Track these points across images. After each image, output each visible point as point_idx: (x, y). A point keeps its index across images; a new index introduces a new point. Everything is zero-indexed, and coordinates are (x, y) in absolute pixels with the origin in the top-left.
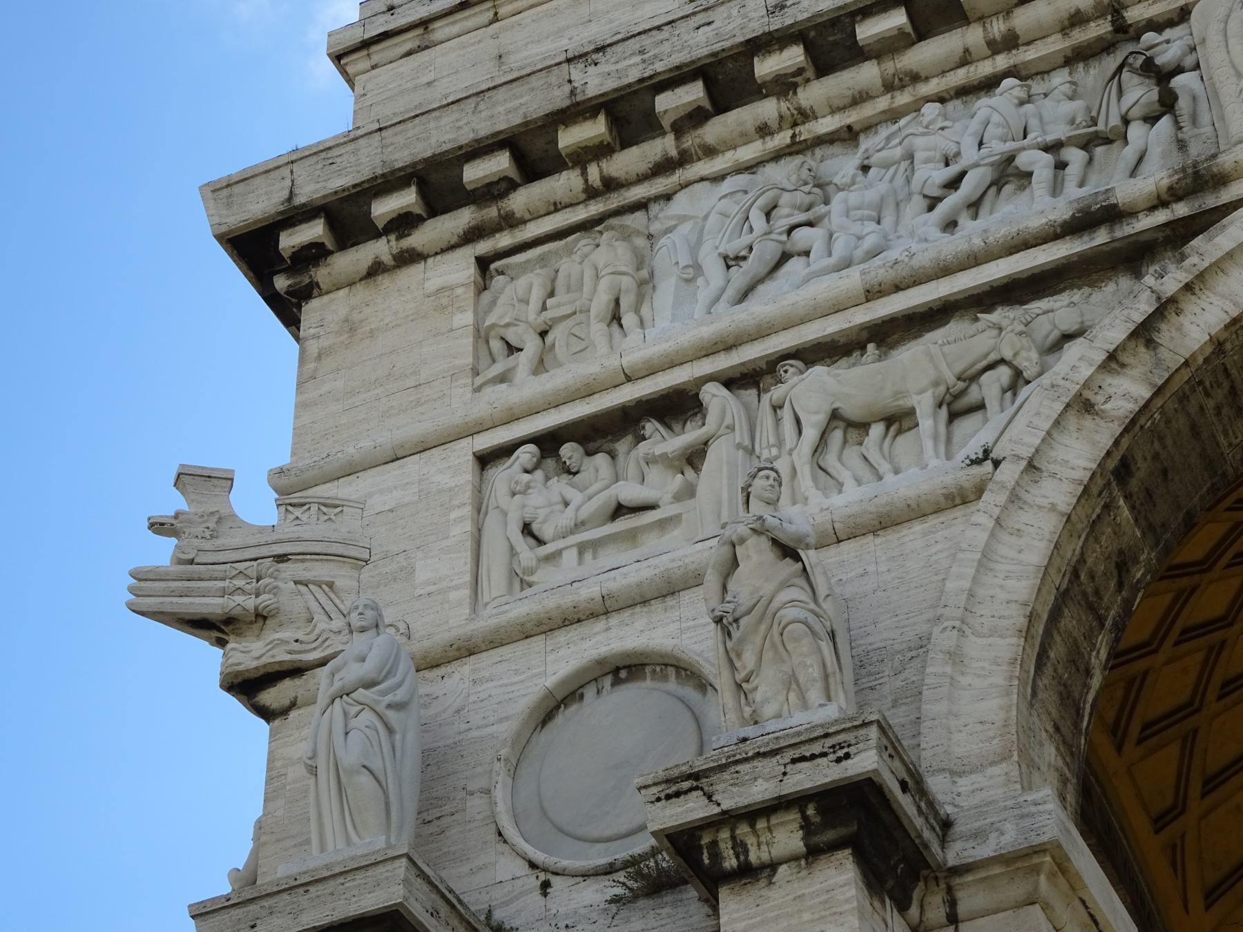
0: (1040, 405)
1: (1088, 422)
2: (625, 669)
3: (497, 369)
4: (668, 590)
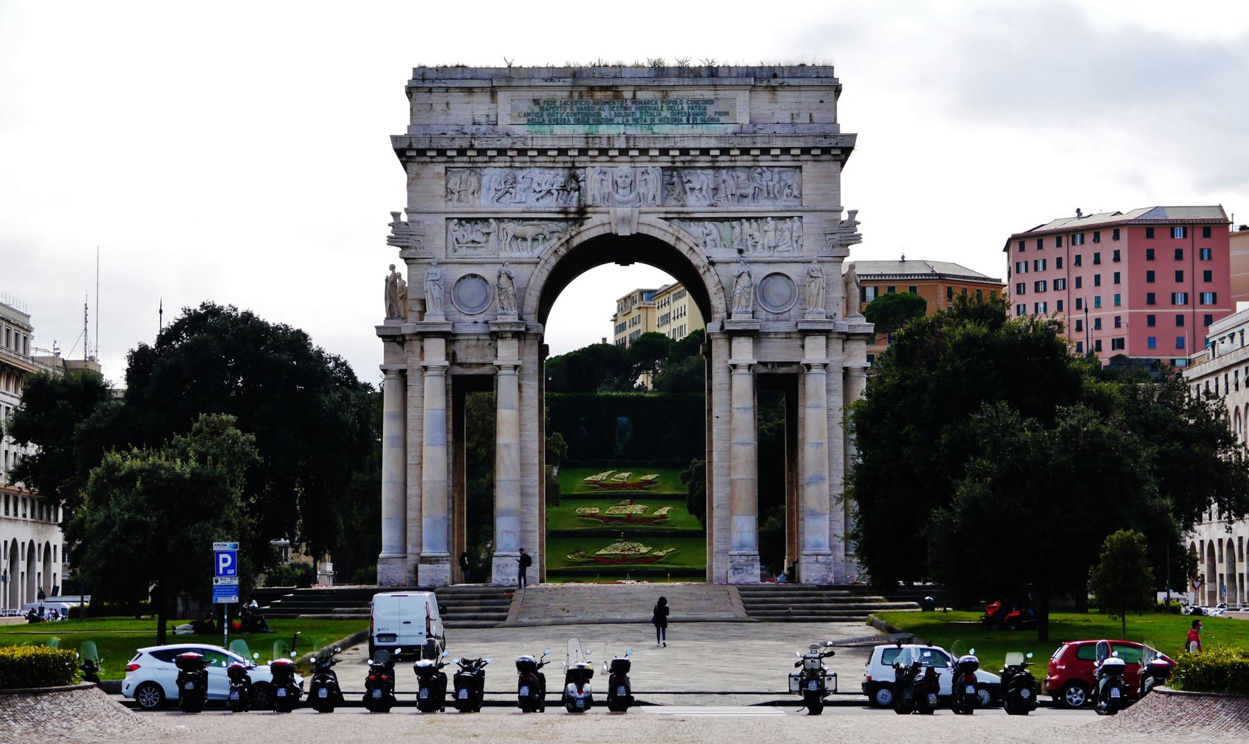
2: (474, 276)
4: (482, 263)
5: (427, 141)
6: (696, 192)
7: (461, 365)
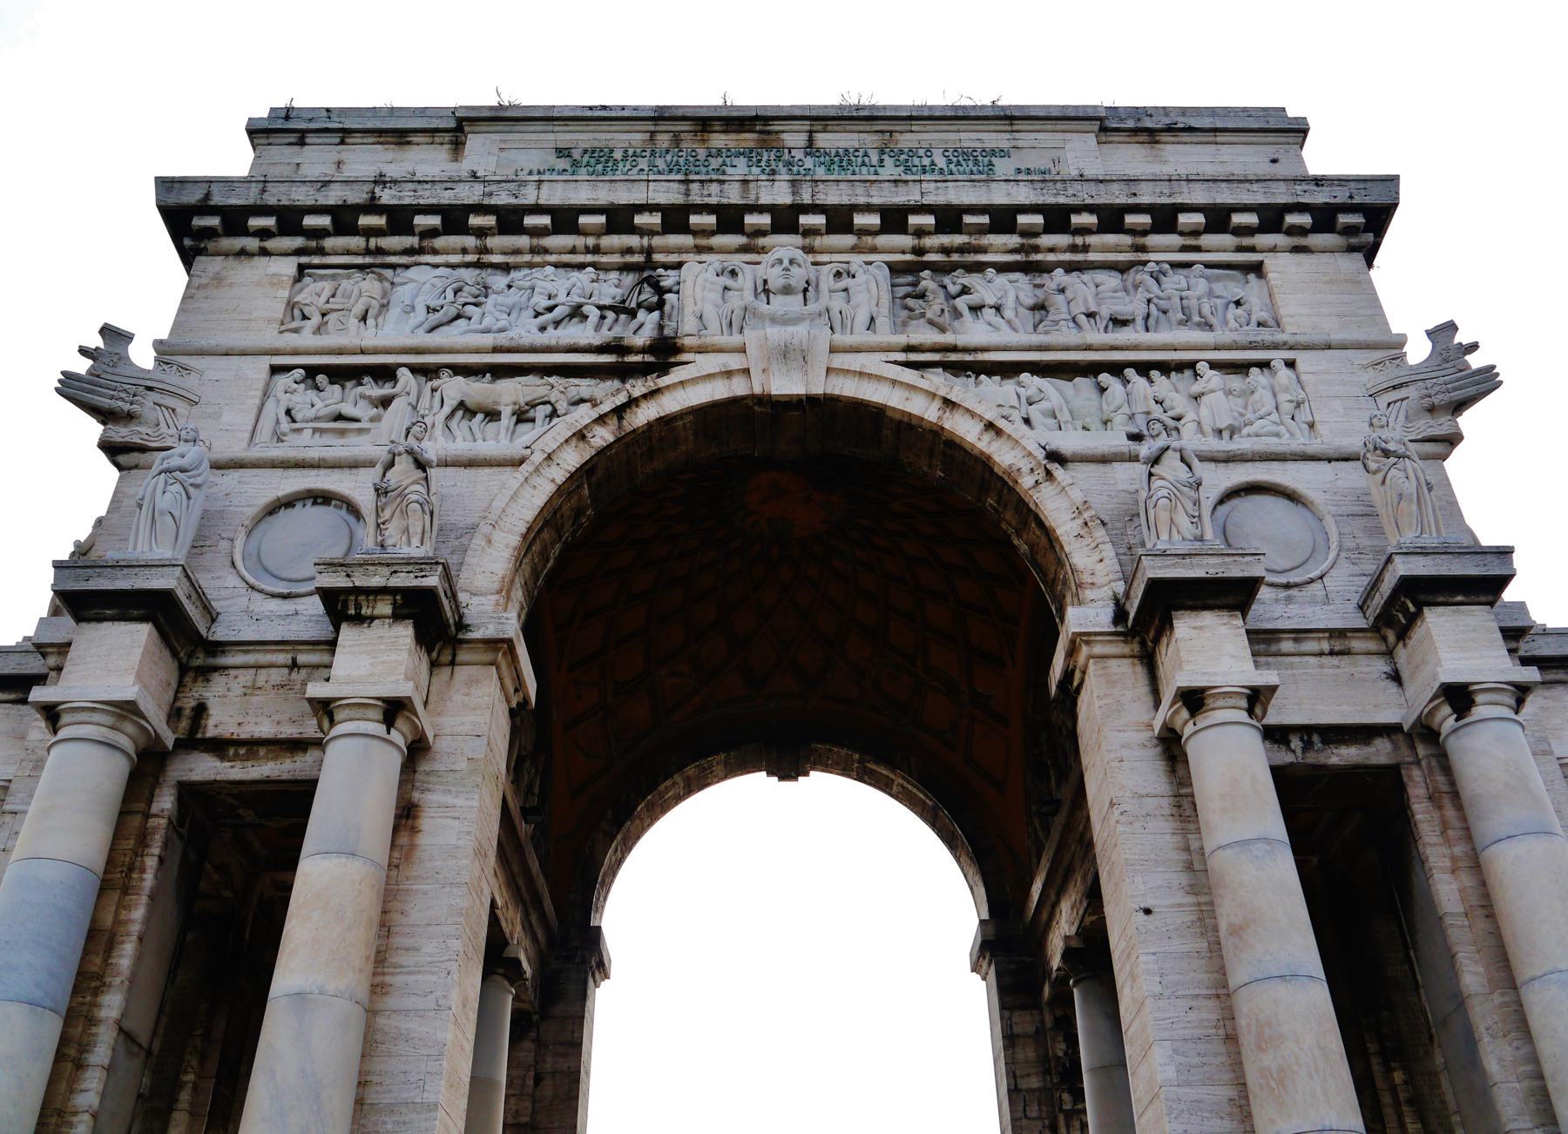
0: (563, 428)
1: (581, 445)
2: (322, 498)
3: (295, 325)
4: (354, 465)
5: (255, 189)
6: (989, 313)
7: (220, 747)
